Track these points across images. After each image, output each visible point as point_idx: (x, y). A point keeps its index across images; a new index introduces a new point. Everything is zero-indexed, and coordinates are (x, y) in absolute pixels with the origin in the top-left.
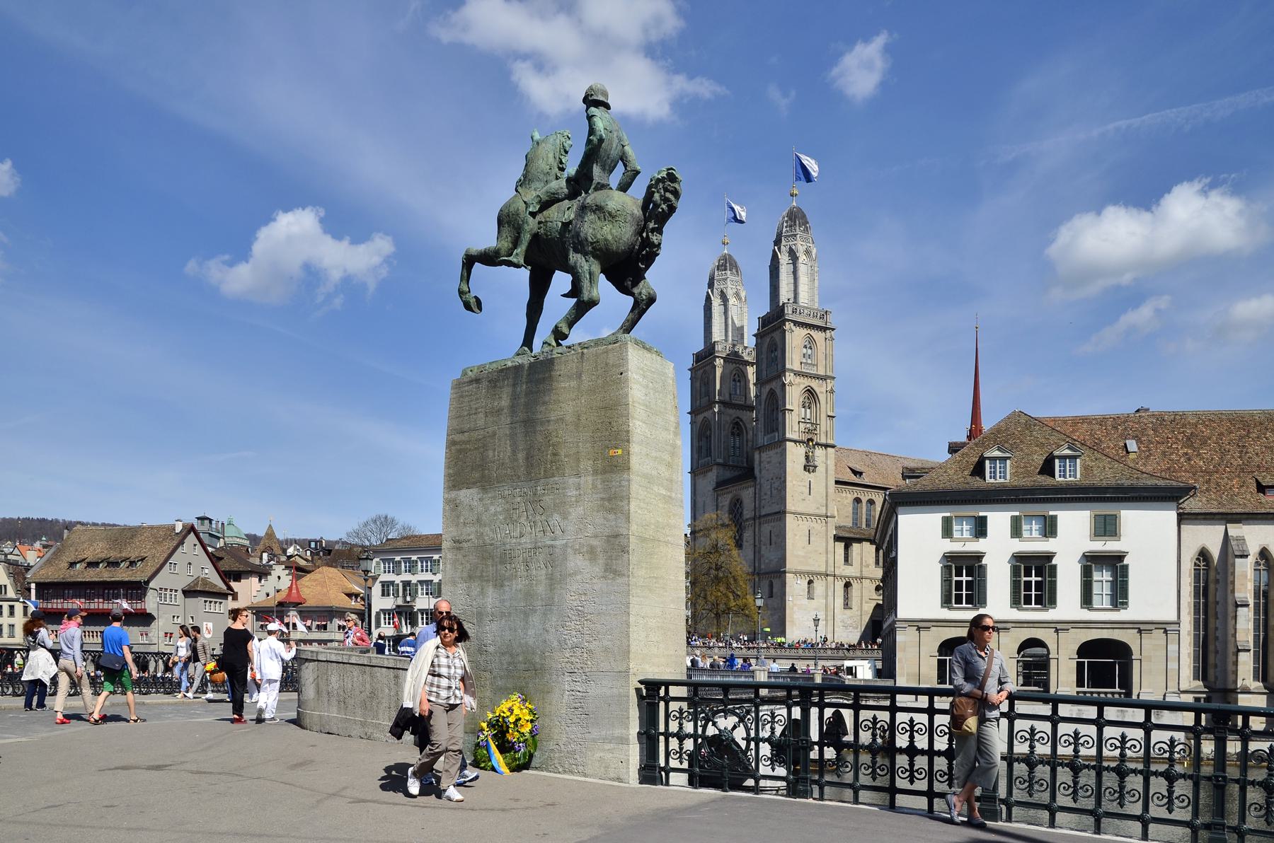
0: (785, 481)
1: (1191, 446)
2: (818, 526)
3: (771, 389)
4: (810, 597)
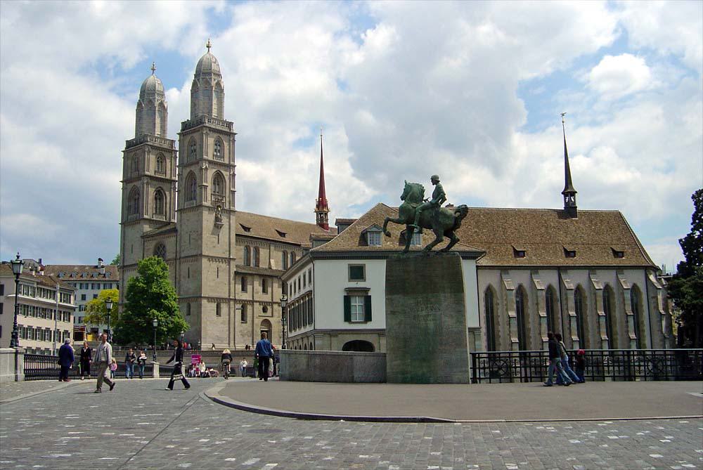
0: (201, 234)
1: (478, 227)
2: (224, 266)
3: (191, 171)
4: (218, 313)
